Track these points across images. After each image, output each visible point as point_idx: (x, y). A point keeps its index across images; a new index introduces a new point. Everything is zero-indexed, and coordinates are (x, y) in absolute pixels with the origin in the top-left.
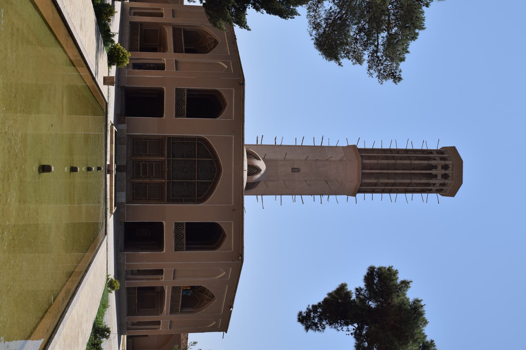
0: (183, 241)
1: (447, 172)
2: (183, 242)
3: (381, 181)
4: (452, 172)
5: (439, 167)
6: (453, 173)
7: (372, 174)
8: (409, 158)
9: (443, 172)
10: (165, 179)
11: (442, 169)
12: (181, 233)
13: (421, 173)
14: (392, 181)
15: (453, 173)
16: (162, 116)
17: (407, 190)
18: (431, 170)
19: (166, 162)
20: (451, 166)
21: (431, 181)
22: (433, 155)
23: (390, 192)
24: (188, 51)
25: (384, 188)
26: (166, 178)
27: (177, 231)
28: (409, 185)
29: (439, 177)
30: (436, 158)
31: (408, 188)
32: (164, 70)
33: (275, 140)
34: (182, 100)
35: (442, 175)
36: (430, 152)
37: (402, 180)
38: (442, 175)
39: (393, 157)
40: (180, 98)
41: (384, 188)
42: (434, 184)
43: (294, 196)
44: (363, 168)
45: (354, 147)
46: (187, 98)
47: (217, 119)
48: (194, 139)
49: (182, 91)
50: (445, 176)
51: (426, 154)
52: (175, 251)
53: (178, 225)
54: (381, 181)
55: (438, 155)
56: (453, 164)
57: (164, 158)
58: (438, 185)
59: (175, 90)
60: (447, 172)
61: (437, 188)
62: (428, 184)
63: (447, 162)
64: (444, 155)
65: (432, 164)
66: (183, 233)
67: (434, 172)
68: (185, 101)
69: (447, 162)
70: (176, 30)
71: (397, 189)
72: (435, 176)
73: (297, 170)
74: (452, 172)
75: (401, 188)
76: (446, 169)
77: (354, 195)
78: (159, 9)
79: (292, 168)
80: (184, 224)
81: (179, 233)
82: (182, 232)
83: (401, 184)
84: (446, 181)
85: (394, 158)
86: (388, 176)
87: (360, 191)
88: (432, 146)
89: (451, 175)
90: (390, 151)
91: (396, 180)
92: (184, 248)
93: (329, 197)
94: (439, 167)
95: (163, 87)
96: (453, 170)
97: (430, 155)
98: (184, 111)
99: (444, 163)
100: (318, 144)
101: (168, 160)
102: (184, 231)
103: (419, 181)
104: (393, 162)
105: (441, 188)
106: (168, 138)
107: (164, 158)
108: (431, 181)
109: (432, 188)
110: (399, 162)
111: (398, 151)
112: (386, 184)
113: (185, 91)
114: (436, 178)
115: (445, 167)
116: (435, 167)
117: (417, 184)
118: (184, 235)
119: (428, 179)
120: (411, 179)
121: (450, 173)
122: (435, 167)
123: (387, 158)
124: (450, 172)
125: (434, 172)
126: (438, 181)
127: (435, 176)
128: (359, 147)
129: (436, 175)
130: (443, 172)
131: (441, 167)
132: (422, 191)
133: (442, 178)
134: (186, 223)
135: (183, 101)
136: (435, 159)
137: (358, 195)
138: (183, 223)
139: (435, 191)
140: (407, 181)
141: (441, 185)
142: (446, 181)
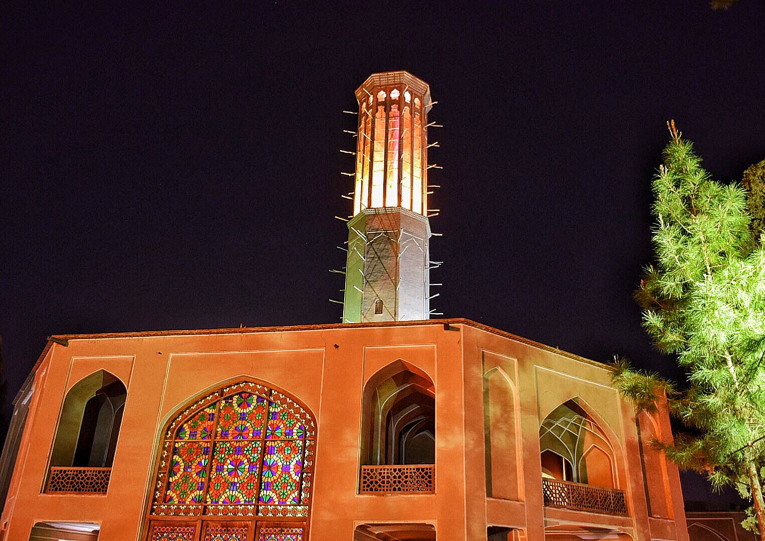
0: (409, 471)
2: (412, 471)
12: (388, 477)
27: (382, 488)
34: (73, 478)
40: (67, 483)
47: (128, 392)
49: (54, 478)
52: (434, 493)
53: (368, 485)
59: (45, 495)
66: (389, 471)
68: (77, 471)
80: (365, 470)
81: (388, 482)
82: (386, 475)
92: (427, 469)
98: (99, 472)
102: (384, 470)
113: (55, 471)
118: (395, 470)
135: (77, 475)
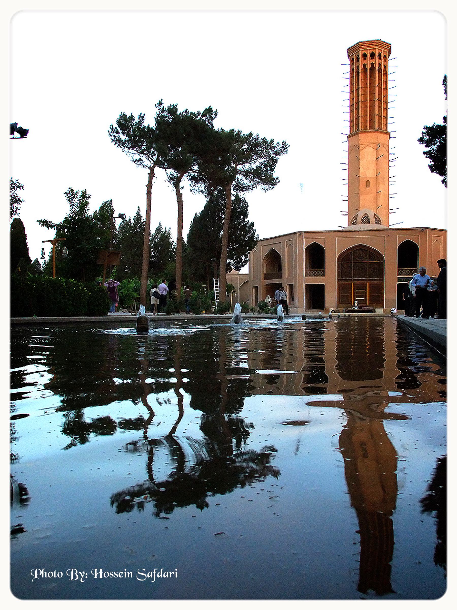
1: (369, 55)
3: (377, 112)
4: (368, 50)
5: (365, 62)
6: (370, 49)
7: (370, 120)
8: (358, 90)
10: (367, 283)
11: (366, 59)
13: (370, 77)
14: (377, 103)
15: (370, 49)
16: (324, 285)
17: (385, 88)
18: (367, 69)
19: (355, 282)
20: (364, 52)
21: (377, 68)
22: (355, 69)
23: (386, 103)
24: (280, 269)
25: (382, 109)
26: (366, 282)
28: (380, 87)
29: (373, 61)
30: (357, 65)
31: (383, 87)
32: (292, 285)
33: (344, 201)
36: (353, 70)
37: (376, 95)
38: (371, 59)
39: (356, 103)
41: (382, 109)
42: (380, 65)
43: (390, 183)
45: (348, 137)
46: (312, 269)
47: (325, 249)
48: (338, 264)
50: (373, 55)
51: (354, 74)
54: (377, 112)
55: (355, 64)
56: (362, 50)
57: (353, 284)
58: (380, 61)
60: (369, 55)
61: (383, 61)
62: (380, 70)
63: (360, 56)
64: (355, 59)
65: (362, 69)
67: (369, 67)
69: (360, 56)
70: (267, 277)
71: (384, 97)
72: (372, 65)
73: (368, 183)
74: (368, 50)
75: (382, 93)
76: (367, 56)
77: (389, 134)
78: (253, 289)
79: (366, 187)
83: (380, 94)
84: (377, 55)
85: (357, 103)
86: (372, 107)
87: (386, 130)
88: (347, 69)
89: (371, 51)
90: (351, 106)
91: (376, 100)
93: (390, 154)
94: (365, 62)
95: (304, 285)
96: (367, 50)
97: (355, 71)
99: (361, 59)
100: (346, 167)
101: (353, 281)
103: (377, 79)
104: (360, 104)
105: (383, 59)
106: (338, 281)
107: (353, 284)
108: (377, 68)
109: (383, 66)
110: (360, 99)
111: (352, 99)
112: (380, 107)
114: (374, 63)
115: (365, 56)
116: (365, 66)
117: (380, 79)
119: (375, 71)
120: (375, 87)
121: (370, 52)
122: (365, 66)
123: (357, 109)
124: (368, 52)
125: (369, 67)
126: (377, 61)
127: (372, 65)
128: (348, 133)
129: (371, 64)
131: (364, 61)
132: (386, 74)
133: (374, 59)
134: (398, 268)
136: (358, 67)
137: (389, 130)
138: (398, 270)
139: (386, 63)
140: (377, 89)
142: (377, 55)
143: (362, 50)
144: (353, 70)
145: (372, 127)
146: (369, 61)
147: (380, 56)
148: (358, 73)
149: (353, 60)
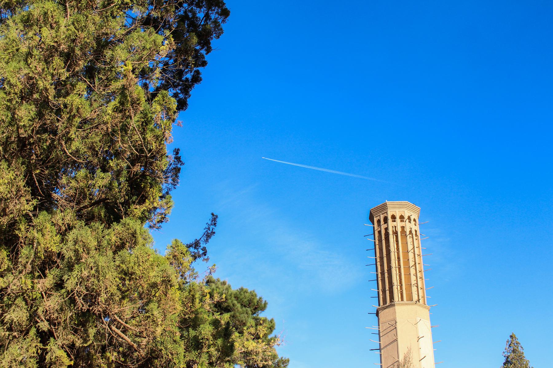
9: (398, 220)
29: (403, 224)
35: (401, 221)
38: (401, 221)
44: (402, 300)
50: (402, 217)
67: (399, 230)
72: (403, 228)
84: (406, 217)
86: (408, 275)
115: (394, 217)
125: (399, 230)
127: (403, 228)
130: (398, 220)
136: (386, 229)
141: (410, 222)
142: (406, 217)
143: (390, 211)
144: (380, 232)
145: (410, 299)
146: (399, 224)
147: (409, 218)
148: (387, 234)
149: (379, 221)
